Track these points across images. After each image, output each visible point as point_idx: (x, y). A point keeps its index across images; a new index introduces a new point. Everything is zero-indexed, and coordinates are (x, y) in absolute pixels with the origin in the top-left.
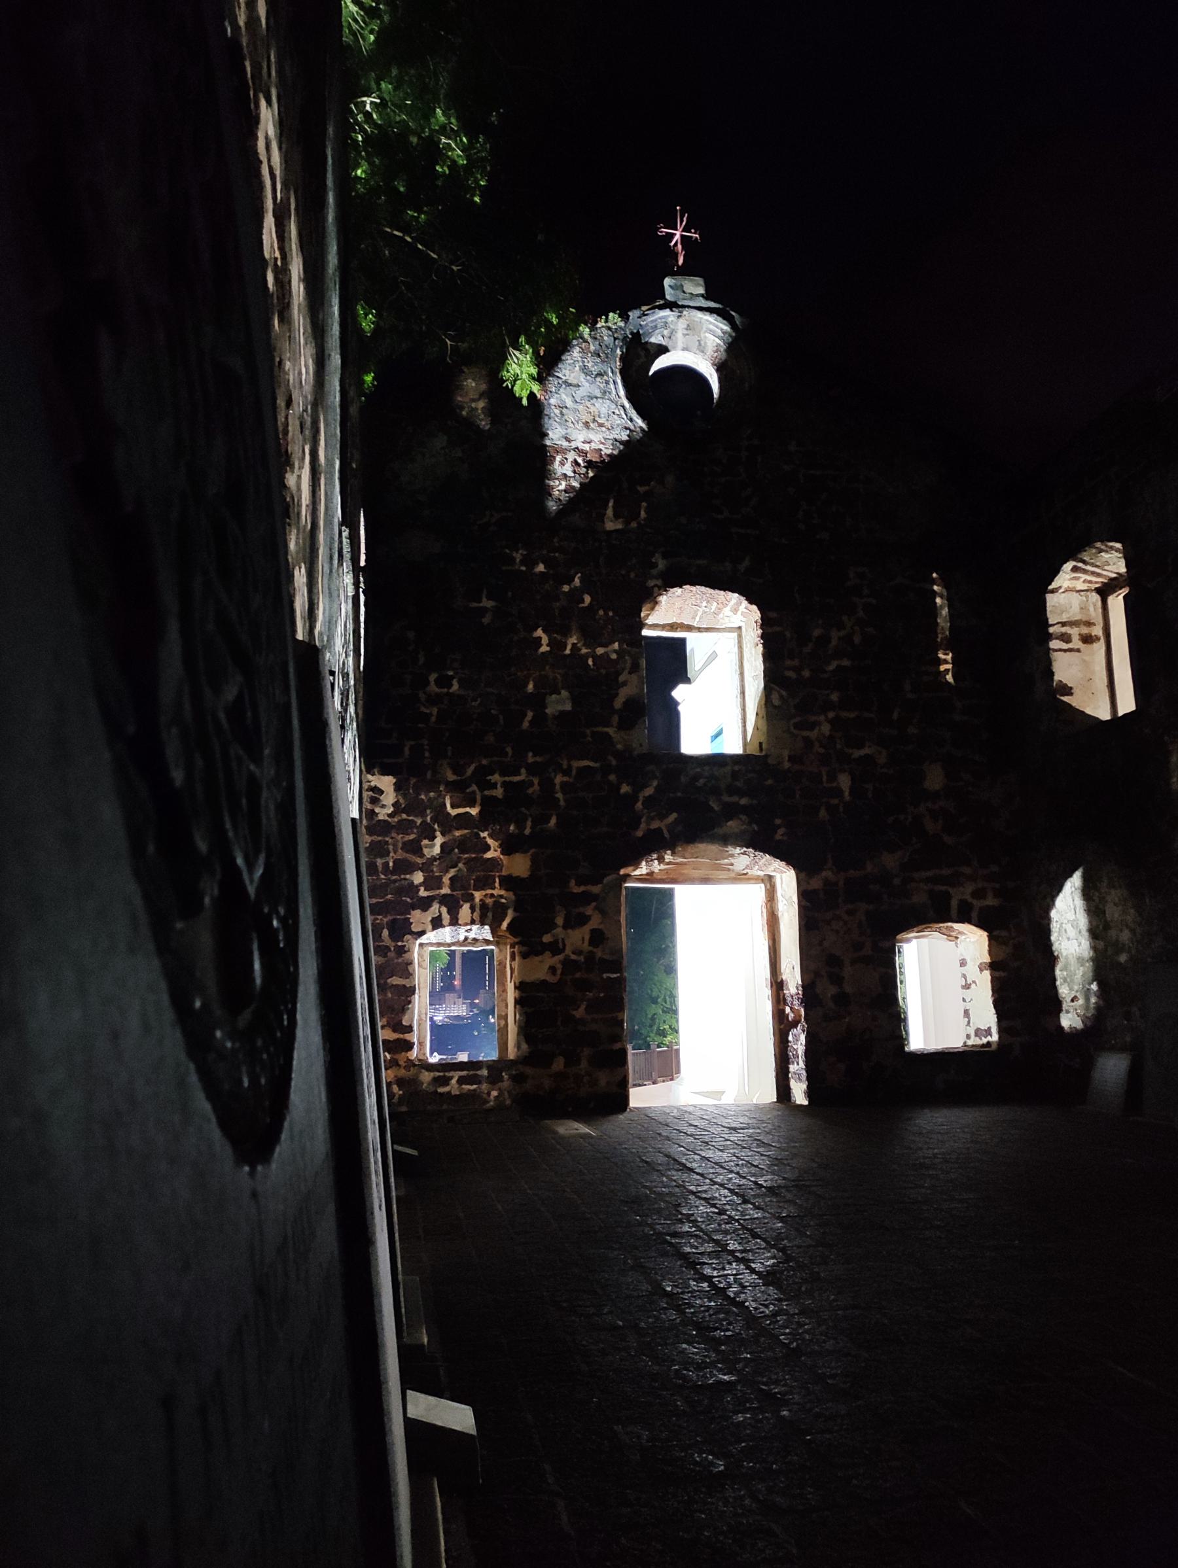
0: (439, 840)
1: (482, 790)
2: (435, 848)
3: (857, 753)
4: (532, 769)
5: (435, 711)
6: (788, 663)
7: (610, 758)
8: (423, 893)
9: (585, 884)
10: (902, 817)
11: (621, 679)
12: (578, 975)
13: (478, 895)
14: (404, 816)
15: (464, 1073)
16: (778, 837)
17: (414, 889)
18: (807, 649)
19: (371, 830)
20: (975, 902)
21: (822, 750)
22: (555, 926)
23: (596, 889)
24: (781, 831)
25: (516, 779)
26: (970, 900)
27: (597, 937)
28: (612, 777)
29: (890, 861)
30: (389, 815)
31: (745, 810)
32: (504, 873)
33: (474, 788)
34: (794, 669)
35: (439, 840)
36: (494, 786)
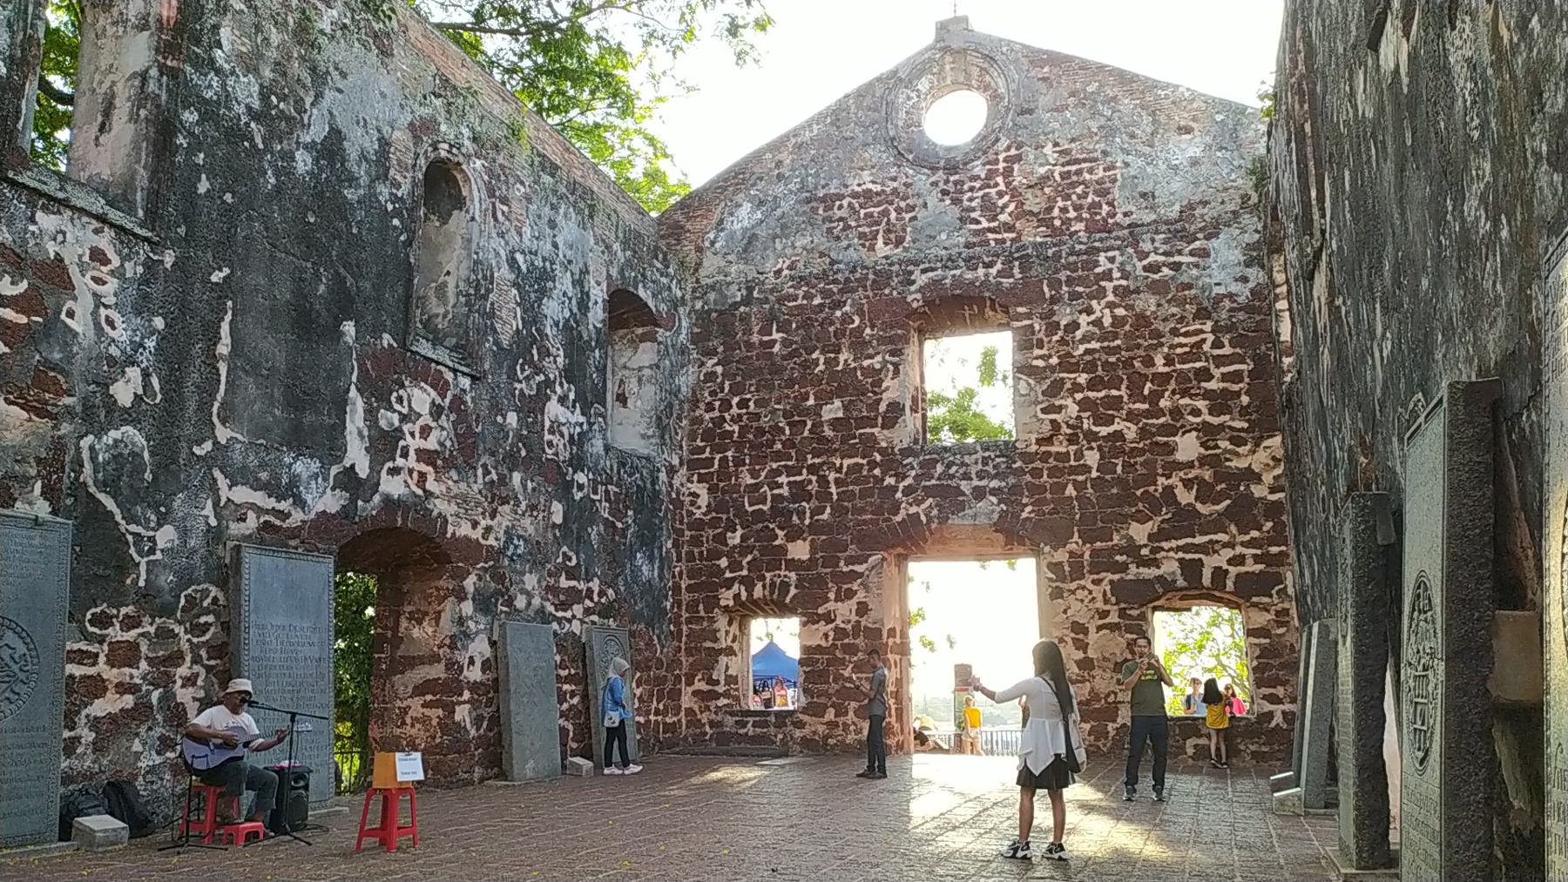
0: (739, 532)
2: (735, 539)
3: (1104, 431)
4: (813, 469)
5: (736, 428)
6: (1037, 352)
8: (728, 575)
10: (1151, 489)
13: (768, 575)
16: (1024, 515)
18: (1055, 338)
20: (1231, 568)
21: (1069, 431)
23: (859, 568)
24: (1029, 508)
25: (798, 478)
26: (1225, 567)
27: (863, 609)
28: (877, 472)
29: (1140, 532)
31: (994, 492)
35: (739, 532)
36: (780, 486)
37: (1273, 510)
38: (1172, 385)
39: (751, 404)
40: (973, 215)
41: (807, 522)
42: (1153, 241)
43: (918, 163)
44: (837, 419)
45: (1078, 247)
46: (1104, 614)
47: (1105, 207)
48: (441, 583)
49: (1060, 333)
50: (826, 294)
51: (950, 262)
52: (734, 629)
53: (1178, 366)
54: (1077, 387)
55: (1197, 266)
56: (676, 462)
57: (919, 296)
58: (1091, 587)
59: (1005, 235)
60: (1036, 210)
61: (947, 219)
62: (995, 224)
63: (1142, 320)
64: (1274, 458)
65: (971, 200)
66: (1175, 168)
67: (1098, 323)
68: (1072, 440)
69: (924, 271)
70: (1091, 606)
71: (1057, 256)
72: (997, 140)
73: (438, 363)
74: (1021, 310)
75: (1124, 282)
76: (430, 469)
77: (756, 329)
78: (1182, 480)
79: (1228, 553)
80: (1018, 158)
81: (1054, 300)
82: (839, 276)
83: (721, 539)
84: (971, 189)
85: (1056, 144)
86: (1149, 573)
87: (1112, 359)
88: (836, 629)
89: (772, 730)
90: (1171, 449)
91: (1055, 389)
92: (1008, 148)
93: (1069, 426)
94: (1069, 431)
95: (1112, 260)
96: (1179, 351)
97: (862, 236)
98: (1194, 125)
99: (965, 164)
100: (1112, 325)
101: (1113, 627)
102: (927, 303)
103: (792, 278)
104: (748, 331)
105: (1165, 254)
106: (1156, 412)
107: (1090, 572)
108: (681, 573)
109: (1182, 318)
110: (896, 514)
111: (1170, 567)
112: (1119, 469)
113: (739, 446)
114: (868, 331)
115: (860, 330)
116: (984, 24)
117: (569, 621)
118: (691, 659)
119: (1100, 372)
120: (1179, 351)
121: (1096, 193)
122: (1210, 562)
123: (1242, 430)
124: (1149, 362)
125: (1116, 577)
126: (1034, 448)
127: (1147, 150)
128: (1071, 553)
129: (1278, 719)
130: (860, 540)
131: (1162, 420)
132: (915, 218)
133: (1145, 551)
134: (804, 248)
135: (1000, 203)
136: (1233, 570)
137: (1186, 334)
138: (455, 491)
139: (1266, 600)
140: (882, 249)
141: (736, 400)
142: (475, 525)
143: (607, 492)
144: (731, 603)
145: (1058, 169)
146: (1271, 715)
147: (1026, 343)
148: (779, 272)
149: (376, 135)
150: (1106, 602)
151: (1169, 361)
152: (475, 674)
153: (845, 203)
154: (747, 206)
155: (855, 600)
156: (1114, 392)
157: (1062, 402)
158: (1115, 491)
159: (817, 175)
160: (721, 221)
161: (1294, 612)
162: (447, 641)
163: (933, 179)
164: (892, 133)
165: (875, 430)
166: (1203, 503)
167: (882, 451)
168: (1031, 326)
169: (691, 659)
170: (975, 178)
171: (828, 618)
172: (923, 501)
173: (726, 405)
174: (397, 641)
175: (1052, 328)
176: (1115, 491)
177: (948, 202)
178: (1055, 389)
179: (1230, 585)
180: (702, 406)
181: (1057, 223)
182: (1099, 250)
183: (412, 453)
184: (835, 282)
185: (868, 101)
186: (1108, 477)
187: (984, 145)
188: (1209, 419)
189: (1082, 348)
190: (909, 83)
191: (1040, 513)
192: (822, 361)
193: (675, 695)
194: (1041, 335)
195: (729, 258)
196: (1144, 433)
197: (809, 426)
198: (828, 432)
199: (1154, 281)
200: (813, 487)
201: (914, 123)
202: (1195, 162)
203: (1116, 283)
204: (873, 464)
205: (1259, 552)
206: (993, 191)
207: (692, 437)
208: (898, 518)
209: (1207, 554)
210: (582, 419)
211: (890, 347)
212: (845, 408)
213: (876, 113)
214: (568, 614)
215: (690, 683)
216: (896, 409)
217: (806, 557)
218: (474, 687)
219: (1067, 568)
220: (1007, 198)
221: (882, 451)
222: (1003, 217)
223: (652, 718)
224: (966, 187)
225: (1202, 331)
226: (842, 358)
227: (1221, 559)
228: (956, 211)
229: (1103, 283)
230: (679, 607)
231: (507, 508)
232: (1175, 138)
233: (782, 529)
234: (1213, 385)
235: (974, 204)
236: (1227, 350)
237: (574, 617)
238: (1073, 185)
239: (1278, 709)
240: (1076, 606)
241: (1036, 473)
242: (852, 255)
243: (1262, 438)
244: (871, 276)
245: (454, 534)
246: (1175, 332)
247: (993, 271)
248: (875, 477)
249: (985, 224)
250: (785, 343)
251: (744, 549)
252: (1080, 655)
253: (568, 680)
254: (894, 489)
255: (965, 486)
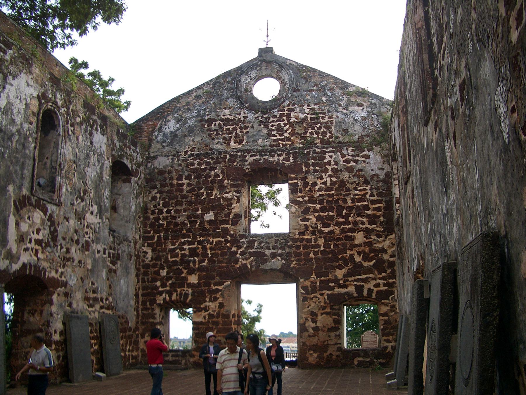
0: (165, 271)
1: (181, 251)
2: (164, 273)
3: (326, 230)
4: (200, 243)
5: (165, 223)
6: (299, 194)
7: (228, 237)
8: (160, 289)
9: (217, 286)
11: (233, 206)
12: (214, 319)
13: (179, 290)
14: (154, 261)
15: (173, 353)
16: (292, 265)
17: (157, 288)
18: (307, 189)
19: (143, 267)
20: (375, 289)
21: (312, 229)
22: (206, 301)
23: (220, 288)
25: (193, 246)
26: (372, 288)
27: (221, 305)
28: (228, 245)
29: (340, 274)
30: (150, 261)
31: (280, 255)
32: (189, 282)
33: (178, 250)
34: (301, 197)
35: (165, 271)
36: (185, 250)
37: (392, 265)
38: (354, 212)
39: (172, 212)
40: (273, 133)
41: (197, 266)
42: (347, 150)
43: (250, 109)
44: (211, 220)
45: (317, 150)
46: (324, 308)
47: (329, 134)
48: (44, 297)
49: (309, 187)
50: (207, 163)
51: (262, 152)
52: (163, 313)
53: (357, 204)
54: (315, 211)
55: (364, 162)
56: (138, 237)
57: (249, 167)
58: (319, 296)
59: (287, 142)
60: (300, 132)
61: (262, 134)
62: (283, 137)
63: (342, 183)
64: (392, 244)
65: (272, 126)
66: (356, 120)
67: (325, 183)
68: (313, 233)
69: (251, 156)
70: (319, 304)
71: (308, 153)
72: (284, 101)
73: (44, 200)
74: (292, 175)
75: (336, 167)
76: (40, 247)
77: (175, 178)
78: (357, 252)
79: (374, 282)
80: (293, 110)
81: (307, 172)
82: (215, 156)
83: (158, 273)
84: (273, 121)
85: (309, 105)
86: (344, 290)
87: (330, 199)
88: (210, 315)
89: (180, 358)
90: (352, 239)
91: (306, 211)
92: (289, 105)
93: (312, 227)
94: (312, 229)
95: (331, 157)
96: (357, 197)
97: (224, 138)
98: (364, 103)
99: (270, 110)
100: (331, 184)
101: (327, 313)
102: (253, 170)
103: (192, 155)
104: (171, 179)
105: (352, 156)
106: (347, 223)
107: (319, 290)
108: (139, 288)
109: (358, 184)
110: (237, 263)
111: (351, 289)
112: (332, 246)
113: (166, 231)
114: (226, 181)
115: (222, 181)
116: (278, 51)
117: (94, 312)
118: (143, 327)
119: (325, 204)
120: (357, 197)
121: (325, 127)
122: (367, 286)
123: (381, 231)
124: (345, 201)
125: (329, 292)
126: (297, 236)
127: (345, 111)
128: (312, 282)
129: (389, 349)
130: (220, 275)
131: (350, 226)
132: (248, 132)
133: (341, 282)
134: (198, 142)
135: (285, 128)
136: (375, 289)
137: (360, 190)
138: (49, 257)
139: (388, 301)
140: (232, 143)
141: (165, 209)
142: (57, 271)
143: (109, 253)
144: (162, 302)
145: (309, 116)
146: (386, 347)
147: (293, 190)
148: (187, 152)
149: (24, 102)
150: (325, 303)
151: (353, 201)
152: (56, 337)
153: (217, 123)
154: (173, 121)
155: (218, 301)
156: (331, 214)
157: (310, 217)
158: (330, 256)
159: (205, 110)
160: (161, 127)
161: (397, 306)
162: (46, 323)
163: (257, 115)
164: (239, 94)
165: (228, 226)
166: (365, 261)
167: (231, 236)
168: (297, 183)
169: (143, 327)
170: (275, 117)
171: (206, 309)
172: (249, 258)
173: (161, 212)
174: (23, 323)
175: (306, 184)
176: (330, 256)
177: (263, 126)
178: (306, 211)
179: (374, 296)
180: (149, 212)
181: (309, 139)
182: (326, 152)
183: (33, 241)
184: (212, 158)
185: (229, 79)
186: (327, 250)
187: (276, 102)
188: (368, 226)
189: (318, 194)
190: (247, 74)
191: (298, 264)
192: (205, 194)
193: (136, 343)
194: (301, 187)
195: (164, 145)
196: (343, 231)
197: (198, 223)
198: (207, 226)
199: (348, 167)
200: (200, 251)
201: (248, 90)
202: (363, 118)
203: (333, 167)
204: (227, 241)
205: (385, 282)
206: (282, 123)
207: (145, 226)
208: (238, 266)
209: (365, 283)
210: (100, 221)
211: (235, 189)
212: (215, 215)
213: (231, 84)
214: (93, 309)
215: (143, 337)
216: (238, 216)
217: (196, 282)
218: (57, 343)
219: (310, 289)
220: (288, 126)
221: (231, 236)
222: (286, 135)
223: (127, 353)
224: (271, 120)
225: (366, 190)
226: (214, 193)
227: (371, 285)
228: (265, 131)
229: (327, 166)
230: (138, 304)
231: (69, 263)
232: (356, 108)
233: (185, 269)
234: (369, 212)
235: (274, 128)
236: (375, 198)
237: (96, 310)
238: (316, 123)
239: (390, 345)
240: (313, 305)
241: (298, 247)
242: (218, 147)
243: (388, 235)
244: (228, 157)
245: (48, 276)
246: (355, 189)
247: (281, 158)
248: (228, 247)
249: (279, 137)
250: (189, 185)
251: (168, 278)
252: (313, 325)
253: (93, 338)
254: (236, 253)
255: (268, 252)
